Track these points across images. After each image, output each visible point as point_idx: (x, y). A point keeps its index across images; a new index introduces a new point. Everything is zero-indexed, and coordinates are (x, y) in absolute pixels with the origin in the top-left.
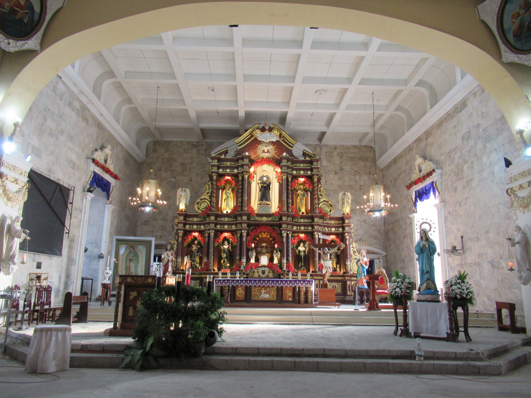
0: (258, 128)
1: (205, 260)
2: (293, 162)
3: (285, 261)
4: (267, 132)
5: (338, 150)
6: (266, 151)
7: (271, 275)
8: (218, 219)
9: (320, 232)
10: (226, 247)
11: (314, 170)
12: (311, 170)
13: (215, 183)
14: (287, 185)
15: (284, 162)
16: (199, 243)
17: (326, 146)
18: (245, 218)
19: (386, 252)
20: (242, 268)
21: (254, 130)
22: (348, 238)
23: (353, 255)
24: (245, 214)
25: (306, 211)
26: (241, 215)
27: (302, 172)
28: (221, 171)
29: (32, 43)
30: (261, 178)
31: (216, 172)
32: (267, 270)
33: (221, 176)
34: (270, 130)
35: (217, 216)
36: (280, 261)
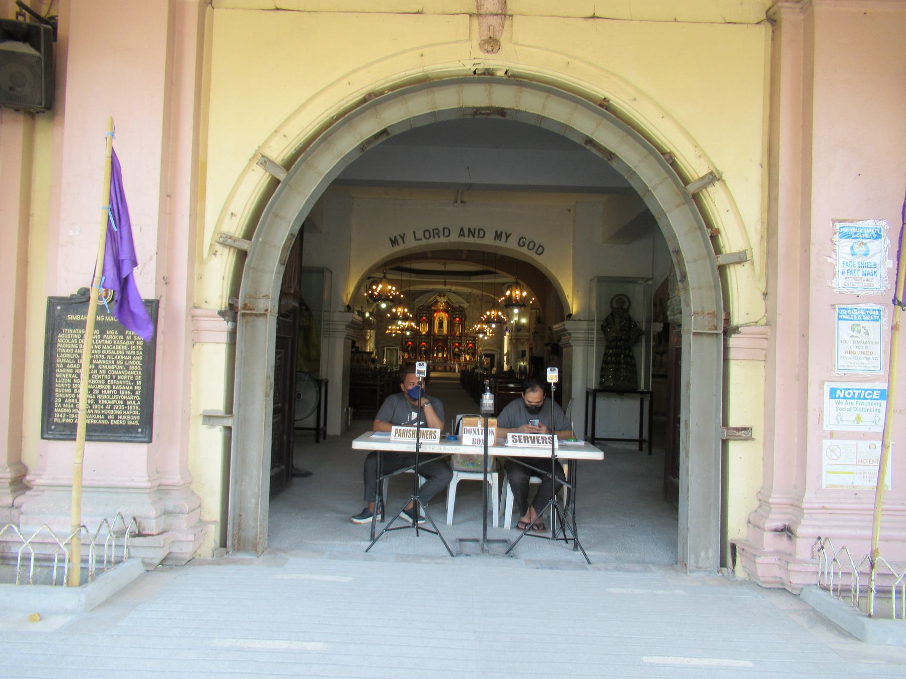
0: (438, 295)
1: (415, 355)
2: (454, 311)
3: (449, 355)
4: (442, 297)
7: (443, 361)
10: (423, 349)
11: (463, 316)
16: (412, 347)
17: (474, 294)
18: (432, 337)
20: (431, 358)
25: (459, 333)
26: (431, 336)
30: (439, 318)
32: (441, 359)
33: (421, 317)
34: (444, 296)
35: (420, 336)
36: (447, 355)
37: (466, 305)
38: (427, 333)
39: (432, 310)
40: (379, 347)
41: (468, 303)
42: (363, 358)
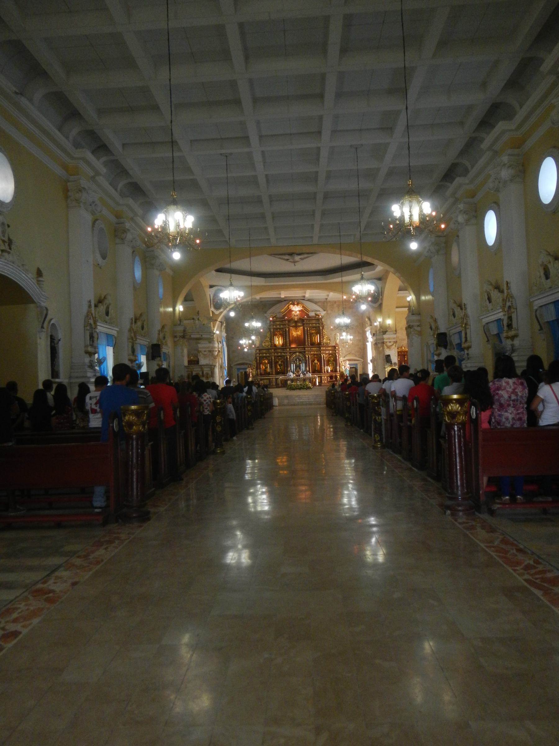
5: (337, 304)
6: (296, 315)
8: (275, 351)
9: (324, 354)
11: (320, 324)
12: (319, 323)
13: (272, 333)
14: (307, 332)
15: (305, 321)
17: (330, 301)
19: (363, 359)
21: (289, 306)
22: (337, 355)
23: (341, 363)
24: (288, 348)
26: (286, 348)
27: (314, 325)
28: (275, 326)
29: (221, 310)
31: (272, 328)
34: (297, 305)
37: (322, 313)
38: (283, 344)
39: (285, 320)
40: (232, 366)
41: (324, 311)
42: (203, 373)
